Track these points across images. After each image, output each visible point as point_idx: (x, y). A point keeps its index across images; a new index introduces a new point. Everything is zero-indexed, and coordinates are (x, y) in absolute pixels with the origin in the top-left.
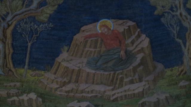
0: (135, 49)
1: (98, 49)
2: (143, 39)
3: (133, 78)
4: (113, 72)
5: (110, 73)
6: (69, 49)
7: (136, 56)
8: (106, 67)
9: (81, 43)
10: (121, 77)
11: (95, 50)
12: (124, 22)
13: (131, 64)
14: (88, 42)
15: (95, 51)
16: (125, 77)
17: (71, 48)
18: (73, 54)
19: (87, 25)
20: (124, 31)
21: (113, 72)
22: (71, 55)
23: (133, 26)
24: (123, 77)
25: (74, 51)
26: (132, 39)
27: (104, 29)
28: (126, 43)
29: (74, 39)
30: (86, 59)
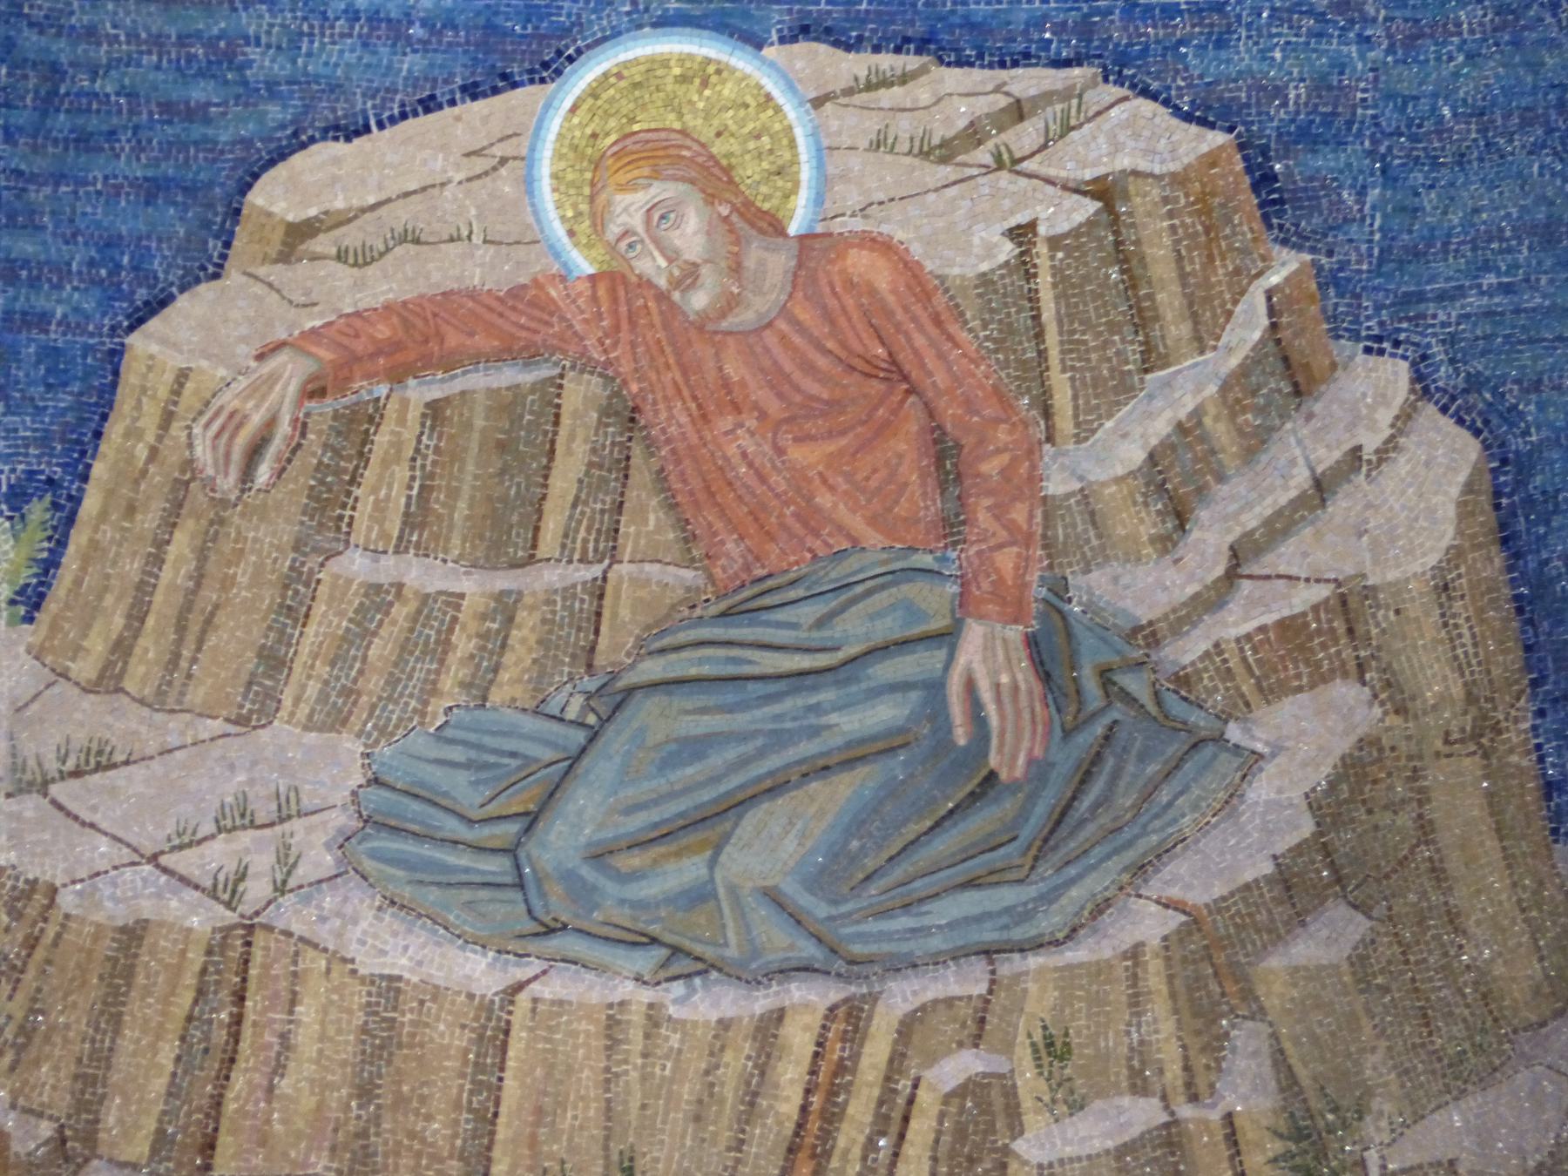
0: (1212, 599)
1: (551, 576)
2: (1371, 443)
3: (1186, 1111)
4: (835, 993)
5: (762, 1002)
6: (49, 565)
7: (1234, 733)
8: (700, 896)
9: (255, 452)
10: (971, 1088)
11: (503, 581)
12: (1018, 111)
13: (1140, 870)
14: (382, 439)
15: (505, 608)
16: (1028, 1081)
17: (79, 538)
18: (122, 648)
19: (353, 130)
20: (1024, 267)
21: (835, 993)
22: (85, 669)
23: (1178, 180)
24: (1011, 1093)
25: (137, 616)
26: (1160, 428)
27: (657, 216)
28: (1056, 485)
29: (131, 376)
30: (350, 745)
